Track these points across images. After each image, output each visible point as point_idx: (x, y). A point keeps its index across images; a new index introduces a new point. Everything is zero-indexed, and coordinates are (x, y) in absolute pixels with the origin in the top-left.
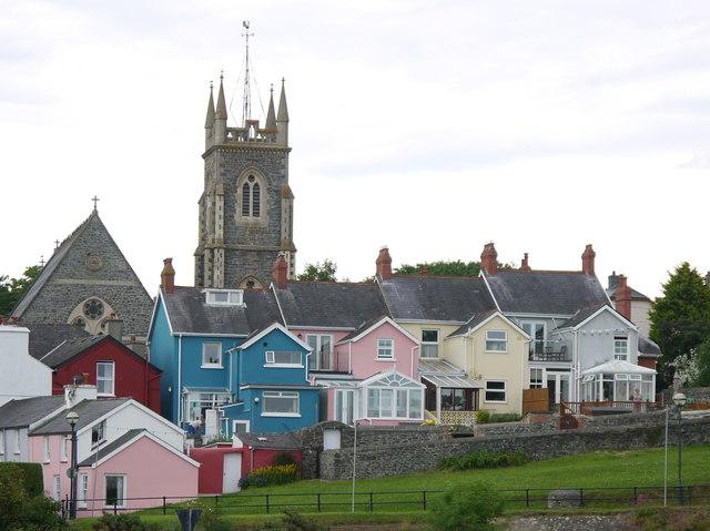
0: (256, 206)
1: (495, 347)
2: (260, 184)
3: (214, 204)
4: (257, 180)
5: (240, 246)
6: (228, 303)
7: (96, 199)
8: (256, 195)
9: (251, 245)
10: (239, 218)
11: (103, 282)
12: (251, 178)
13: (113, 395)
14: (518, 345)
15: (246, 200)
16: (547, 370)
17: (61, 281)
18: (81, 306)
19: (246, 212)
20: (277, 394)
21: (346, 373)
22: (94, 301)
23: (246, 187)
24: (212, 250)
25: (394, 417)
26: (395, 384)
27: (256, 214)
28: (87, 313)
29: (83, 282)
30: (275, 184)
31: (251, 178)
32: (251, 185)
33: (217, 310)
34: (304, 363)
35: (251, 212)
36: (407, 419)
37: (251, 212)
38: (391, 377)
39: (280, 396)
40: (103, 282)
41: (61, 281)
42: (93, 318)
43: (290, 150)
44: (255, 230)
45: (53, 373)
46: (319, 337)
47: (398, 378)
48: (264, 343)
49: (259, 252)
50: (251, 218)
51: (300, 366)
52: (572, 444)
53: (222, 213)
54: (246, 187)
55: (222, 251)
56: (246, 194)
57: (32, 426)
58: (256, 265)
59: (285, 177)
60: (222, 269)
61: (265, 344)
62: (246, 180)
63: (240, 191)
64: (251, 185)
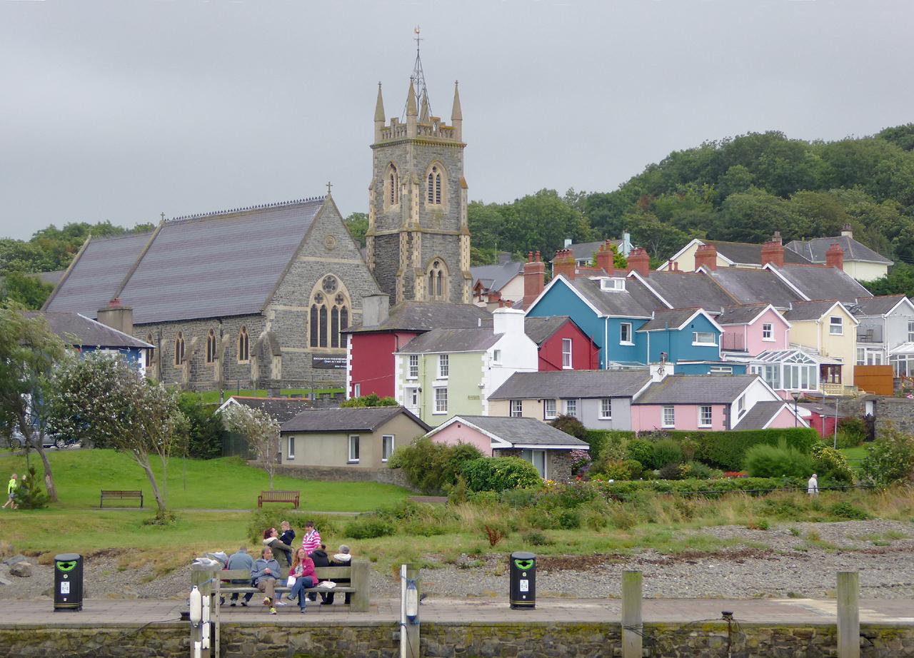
0: (438, 194)
1: (835, 330)
2: (441, 174)
3: (410, 192)
4: (439, 171)
7: (329, 185)
9: (437, 230)
11: (336, 260)
13: (570, 367)
14: (850, 327)
15: (431, 189)
16: (868, 349)
17: (306, 259)
18: (320, 281)
20: (719, 369)
21: (742, 351)
22: (329, 277)
24: (409, 233)
26: (800, 361)
28: (324, 288)
29: (323, 260)
30: (453, 175)
32: (435, 175)
34: (717, 343)
35: (435, 199)
36: (807, 390)
37: (435, 199)
38: (797, 356)
39: (721, 371)
40: (336, 260)
41: (306, 259)
42: (329, 292)
43: (463, 146)
44: (440, 216)
45: (539, 349)
47: (802, 356)
50: (435, 206)
51: (714, 345)
53: (417, 200)
56: (431, 183)
57: (635, 397)
58: (440, 248)
59: (461, 169)
60: (419, 250)
61: (693, 326)
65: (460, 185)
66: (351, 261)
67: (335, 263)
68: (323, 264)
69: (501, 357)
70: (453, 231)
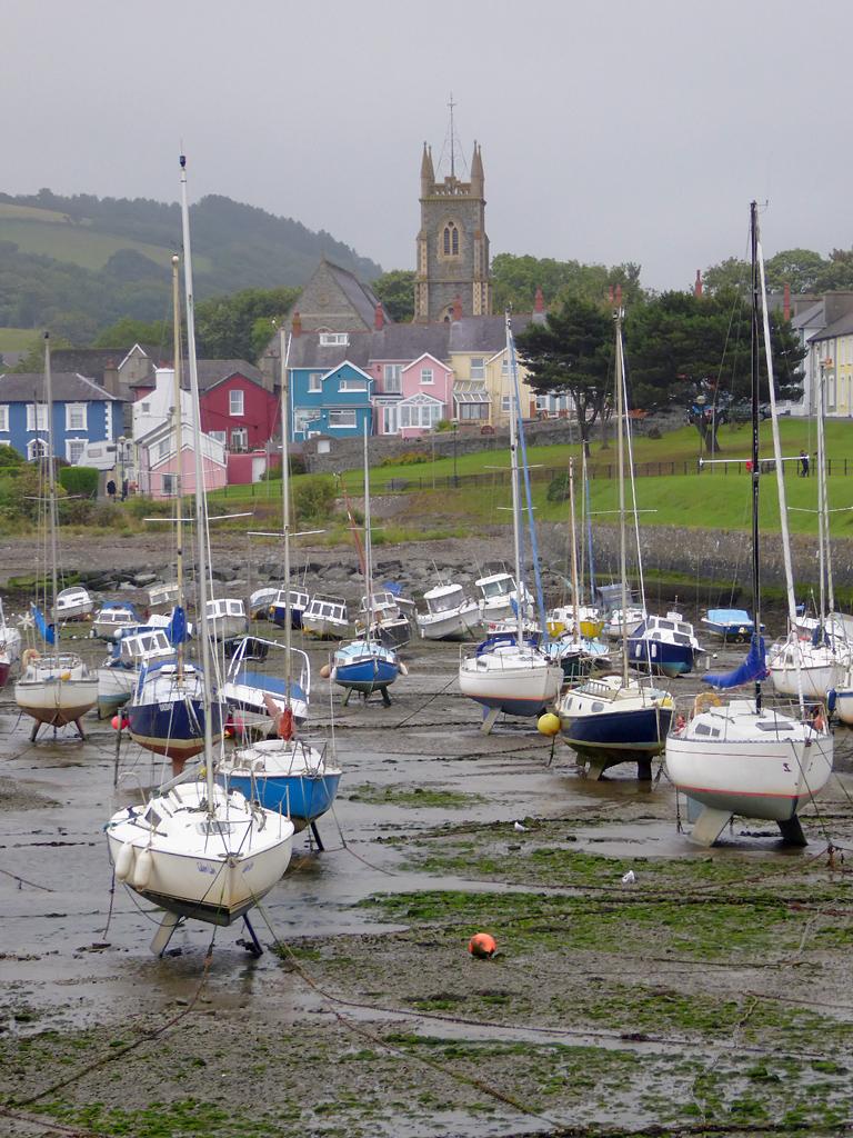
0: (455, 246)
4: (455, 225)
5: (442, 280)
6: (336, 344)
8: (455, 237)
9: (451, 279)
10: (441, 257)
11: (329, 315)
12: (451, 224)
15: (447, 242)
19: (447, 252)
23: (447, 231)
25: (420, 426)
26: (420, 403)
27: (456, 252)
30: (468, 227)
31: (451, 224)
32: (451, 229)
33: (325, 349)
35: (451, 252)
37: (451, 252)
38: (418, 398)
40: (329, 315)
44: (453, 266)
46: (394, 366)
47: (423, 398)
48: (338, 375)
49: (457, 283)
52: (473, 447)
54: (447, 231)
55: (426, 285)
60: (426, 299)
62: (447, 226)
63: (441, 235)
64: (451, 229)
65: (480, 237)
66: (345, 315)
67: (328, 318)
68: (315, 319)
69: (151, 408)
70: (467, 279)
